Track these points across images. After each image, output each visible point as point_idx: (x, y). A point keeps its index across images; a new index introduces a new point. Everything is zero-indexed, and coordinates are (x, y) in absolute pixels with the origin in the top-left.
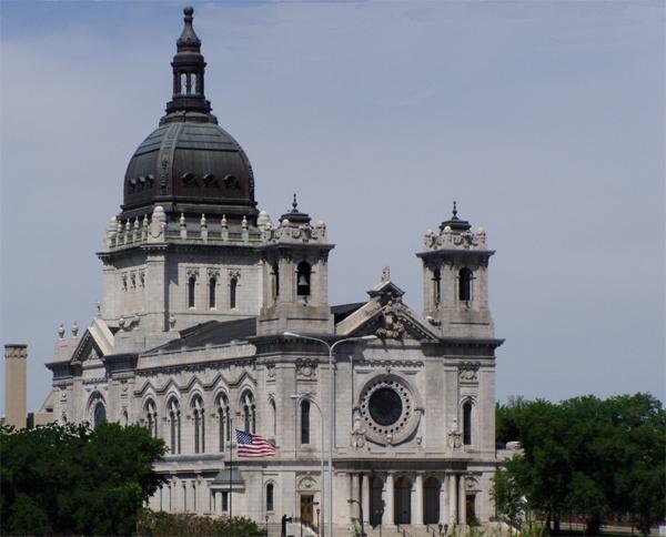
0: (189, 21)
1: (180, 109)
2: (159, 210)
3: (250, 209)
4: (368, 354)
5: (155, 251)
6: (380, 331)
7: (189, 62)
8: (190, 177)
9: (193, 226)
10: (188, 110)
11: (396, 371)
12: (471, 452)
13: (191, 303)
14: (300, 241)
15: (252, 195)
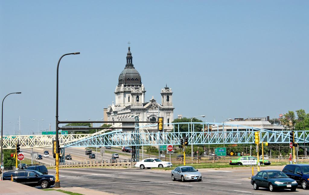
0: (129, 50)
1: (127, 66)
2: (123, 85)
3: (140, 84)
4: (149, 111)
5: (122, 92)
6: (151, 107)
7: (129, 58)
8: (128, 79)
9: (129, 88)
10: (129, 66)
11: (155, 114)
12: (169, 128)
13: (129, 101)
14: (137, 92)
15: (141, 81)
